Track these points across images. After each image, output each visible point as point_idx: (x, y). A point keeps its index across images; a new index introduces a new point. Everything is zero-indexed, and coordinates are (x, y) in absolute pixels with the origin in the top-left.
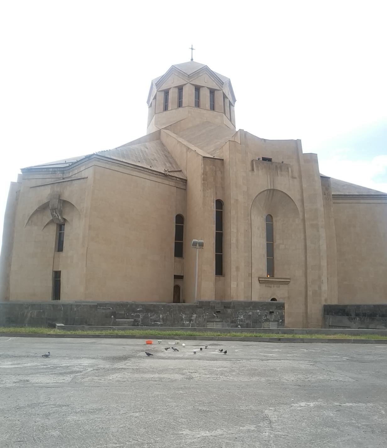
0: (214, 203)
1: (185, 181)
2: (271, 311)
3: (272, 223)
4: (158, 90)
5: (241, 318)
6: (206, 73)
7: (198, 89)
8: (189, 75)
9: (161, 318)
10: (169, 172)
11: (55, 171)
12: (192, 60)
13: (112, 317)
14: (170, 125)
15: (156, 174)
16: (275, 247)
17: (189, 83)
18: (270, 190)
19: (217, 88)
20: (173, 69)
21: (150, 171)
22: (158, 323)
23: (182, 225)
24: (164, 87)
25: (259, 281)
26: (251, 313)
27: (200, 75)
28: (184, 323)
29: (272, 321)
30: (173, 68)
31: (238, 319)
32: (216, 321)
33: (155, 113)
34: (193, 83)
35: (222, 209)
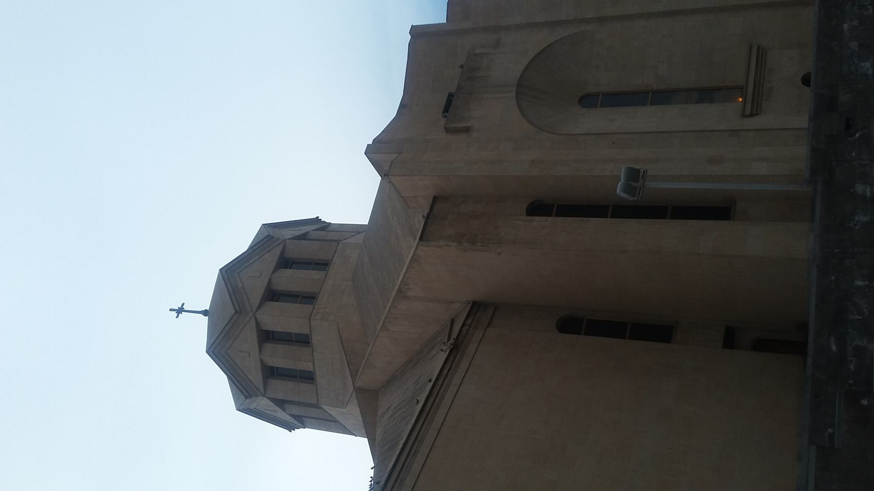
0: (533, 221)
1: (476, 307)
3: (601, 95)
4: (262, 394)
6: (238, 273)
7: (272, 295)
8: (236, 312)
10: (449, 340)
12: (205, 313)
13: (865, 402)
14: (348, 366)
15: (449, 370)
18: (518, 93)
19: (277, 251)
21: (440, 383)
23: (585, 322)
24: (256, 376)
25: (752, 115)
26: (854, 45)
27: (240, 286)
30: (213, 352)
33: (317, 406)
34: (257, 305)
35: (554, 205)
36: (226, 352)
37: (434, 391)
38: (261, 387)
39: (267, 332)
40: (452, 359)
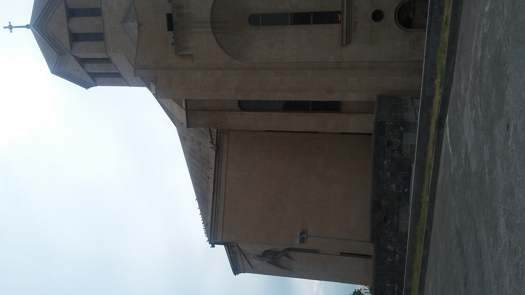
0: (244, 115)
2: (386, 143)
5: (394, 187)
7: (75, 38)
8: (60, 55)
9: (390, 285)
11: (232, 252)
12: (27, 27)
15: (219, 163)
16: (296, 11)
17: (71, 54)
18: (213, 28)
19: (63, 6)
20: (57, 71)
21: (217, 172)
22: (396, 289)
24: (89, 79)
26: (388, 174)
27: (52, 35)
28: (397, 259)
29: (401, 141)
30: (56, 72)
31: (396, 192)
32: (398, 221)
36: (46, 26)
37: (215, 177)
38: (93, 83)
39: (84, 59)
40: (218, 156)
